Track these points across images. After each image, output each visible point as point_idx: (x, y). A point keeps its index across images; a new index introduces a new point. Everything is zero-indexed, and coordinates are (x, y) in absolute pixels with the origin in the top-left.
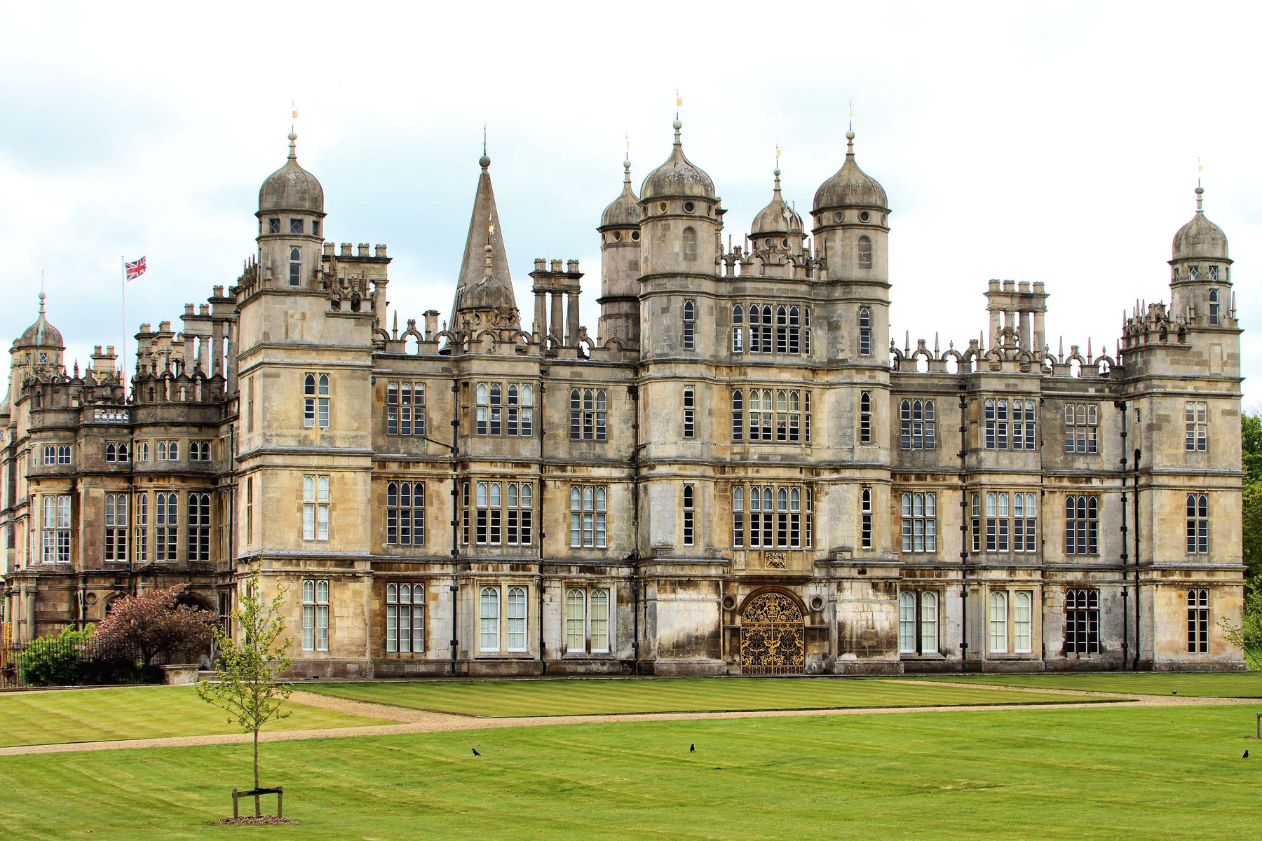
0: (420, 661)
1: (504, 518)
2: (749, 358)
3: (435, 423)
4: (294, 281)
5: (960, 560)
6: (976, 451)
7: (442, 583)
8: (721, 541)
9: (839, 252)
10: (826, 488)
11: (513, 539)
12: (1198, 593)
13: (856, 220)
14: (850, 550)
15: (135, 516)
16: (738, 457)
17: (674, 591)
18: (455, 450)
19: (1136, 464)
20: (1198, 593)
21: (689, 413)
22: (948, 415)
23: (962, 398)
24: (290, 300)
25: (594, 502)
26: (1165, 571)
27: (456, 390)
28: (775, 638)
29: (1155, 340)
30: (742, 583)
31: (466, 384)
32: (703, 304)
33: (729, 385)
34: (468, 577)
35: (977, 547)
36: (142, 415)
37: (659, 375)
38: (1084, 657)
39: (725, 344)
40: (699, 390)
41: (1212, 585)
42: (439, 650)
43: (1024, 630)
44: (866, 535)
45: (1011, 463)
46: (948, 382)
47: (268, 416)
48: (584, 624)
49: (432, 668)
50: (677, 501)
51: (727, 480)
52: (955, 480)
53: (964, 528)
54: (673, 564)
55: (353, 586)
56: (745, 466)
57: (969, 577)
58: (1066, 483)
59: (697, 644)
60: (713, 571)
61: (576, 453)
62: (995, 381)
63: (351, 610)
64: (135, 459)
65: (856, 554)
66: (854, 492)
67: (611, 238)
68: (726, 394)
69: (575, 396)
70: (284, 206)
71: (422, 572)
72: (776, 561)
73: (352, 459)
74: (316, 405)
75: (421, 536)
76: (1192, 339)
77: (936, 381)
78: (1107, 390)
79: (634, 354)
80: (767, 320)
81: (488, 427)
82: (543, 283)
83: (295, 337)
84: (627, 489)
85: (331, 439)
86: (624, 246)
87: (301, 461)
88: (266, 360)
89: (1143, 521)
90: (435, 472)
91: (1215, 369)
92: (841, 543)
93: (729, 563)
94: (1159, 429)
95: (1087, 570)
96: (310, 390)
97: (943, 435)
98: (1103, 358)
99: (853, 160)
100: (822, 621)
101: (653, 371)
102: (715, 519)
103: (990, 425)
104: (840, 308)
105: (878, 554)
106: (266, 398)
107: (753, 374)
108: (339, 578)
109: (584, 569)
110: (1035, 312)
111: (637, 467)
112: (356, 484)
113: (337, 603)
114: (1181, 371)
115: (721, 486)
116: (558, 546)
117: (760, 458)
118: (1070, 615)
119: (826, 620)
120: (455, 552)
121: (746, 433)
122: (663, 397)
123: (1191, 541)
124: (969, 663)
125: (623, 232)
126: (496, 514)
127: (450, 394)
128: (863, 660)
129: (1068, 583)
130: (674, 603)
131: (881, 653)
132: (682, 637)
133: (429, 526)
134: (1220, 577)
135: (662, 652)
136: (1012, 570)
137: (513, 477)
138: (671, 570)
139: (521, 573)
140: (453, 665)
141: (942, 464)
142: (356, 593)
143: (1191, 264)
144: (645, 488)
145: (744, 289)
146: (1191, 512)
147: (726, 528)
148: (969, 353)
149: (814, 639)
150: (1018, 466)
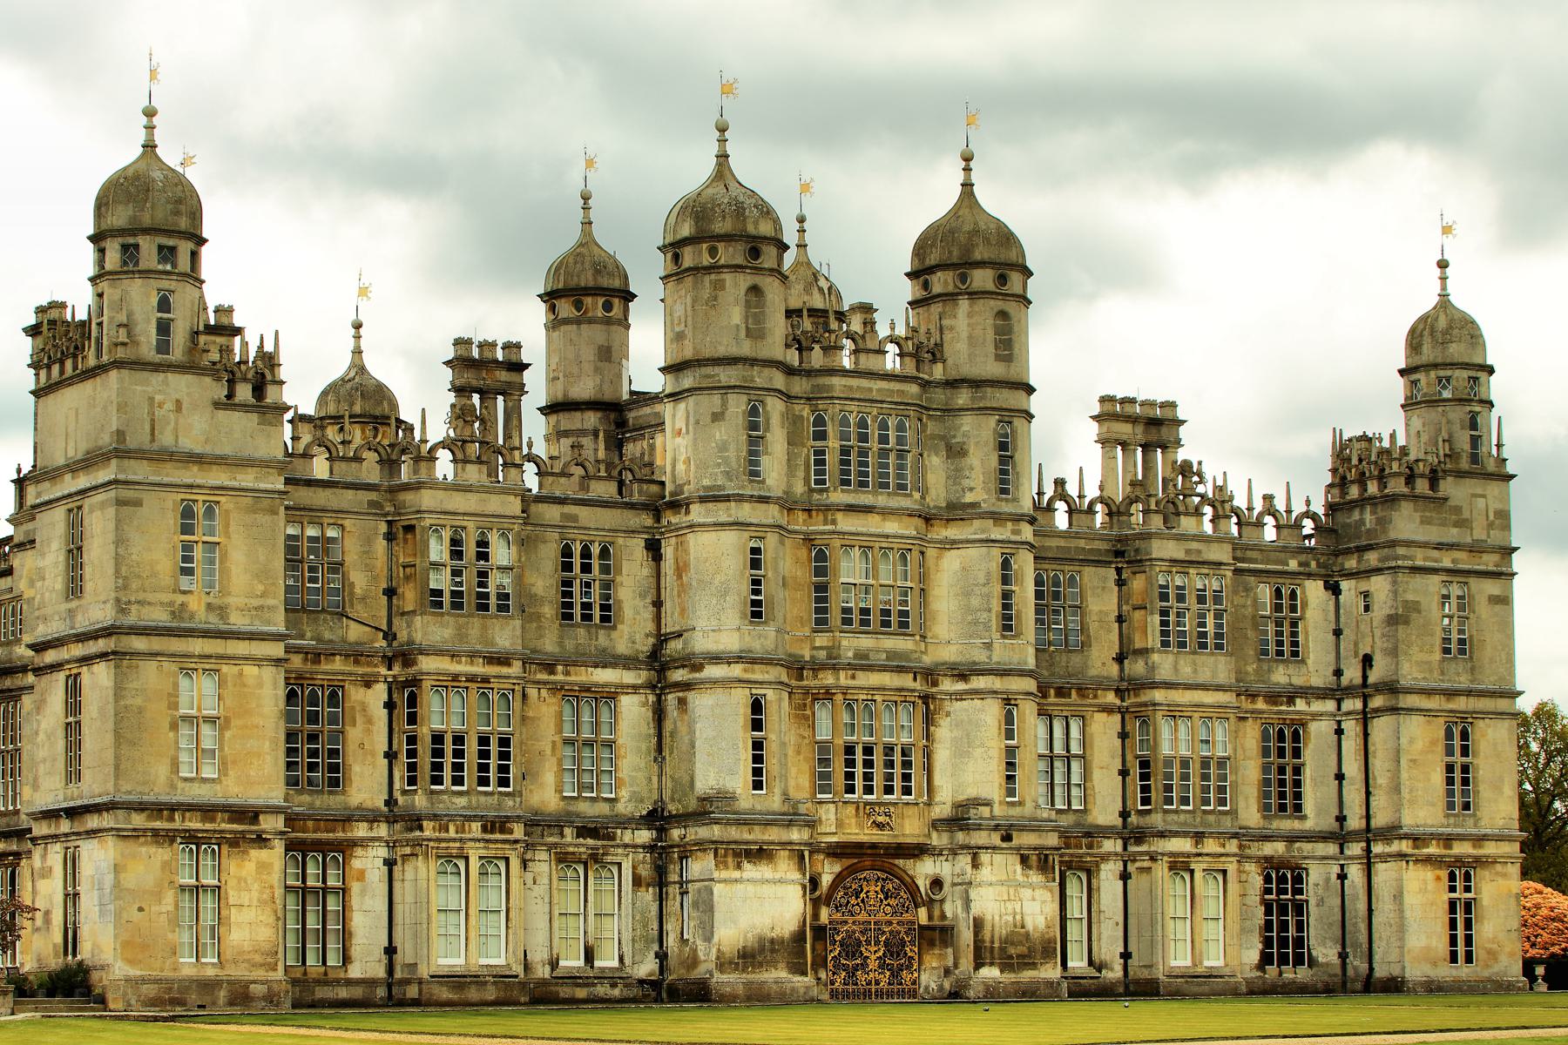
0: (338, 982)
1: (471, 747)
2: (838, 497)
3: (358, 591)
4: (164, 347)
5: (1119, 822)
6: (1144, 652)
7: (371, 852)
8: (798, 787)
9: (964, 335)
10: (949, 706)
11: (484, 781)
12: (1460, 873)
13: (991, 286)
14: (988, 804)
16: (822, 654)
17: (739, 867)
18: (390, 636)
19: (1365, 677)
20: (1460, 873)
21: (756, 582)
22: (1100, 596)
23: (1119, 571)
24: (157, 378)
25: (596, 726)
26: (1417, 839)
27: (390, 537)
28: (877, 943)
29: (1397, 486)
30: (829, 855)
31: (410, 529)
32: (775, 406)
33: (808, 540)
34: (417, 843)
35: (1146, 801)
37: (709, 520)
38: (1289, 974)
39: (801, 474)
40: (771, 543)
41: (1480, 862)
42: (367, 964)
43: (1213, 931)
44: (1010, 778)
45: (1195, 671)
46: (1098, 545)
47: (124, 570)
48: (599, 921)
49: (357, 993)
50: (741, 721)
51: (806, 691)
52: (1111, 698)
53: (1124, 773)
54: (739, 823)
55: (256, 854)
56: (835, 668)
57: (1133, 849)
58: (1260, 705)
59: (773, 951)
60: (795, 835)
61: (570, 645)
62: (1171, 544)
63: (255, 895)
65: (997, 811)
66: (991, 712)
67: (565, 308)
68: (803, 553)
69: (567, 552)
70: (147, 220)
71: (340, 835)
72: (880, 819)
73: (254, 643)
74: (198, 553)
75: (336, 779)
76: (1448, 487)
77: (1082, 543)
78: (1313, 564)
79: (654, 488)
80: (863, 438)
81: (446, 599)
82: (469, 377)
83: (166, 439)
84: (645, 704)
85: (222, 611)
86: (591, 321)
87: (177, 645)
88: (121, 477)
89: (1379, 765)
90: (360, 670)
91: (1479, 533)
92: (971, 792)
93: (812, 824)
94: (1407, 622)
95: (1291, 839)
96: (187, 529)
97: (1093, 627)
98: (1307, 514)
99: (972, 194)
100: (943, 916)
101: (697, 513)
102: (790, 752)
103: (1164, 613)
104: (967, 423)
105: (1028, 810)
106: (120, 541)
107: (846, 523)
108: (234, 843)
109: (584, 831)
110: (1164, 447)
111: (665, 669)
112: (260, 685)
113: (232, 883)
114: (1433, 534)
115: (798, 699)
116: (546, 794)
117: (856, 656)
118: (1268, 912)
119: (949, 914)
120: (390, 802)
121: (835, 617)
122: (712, 553)
123: (1450, 793)
124: (1137, 982)
125: (588, 300)
126: (459, 739)
127: (381, 544)
128: (1009, 977)
129: (1268, 859)
130: (739, 886)
131: (1033, 966)
132: (751, 940)
133: (350, 760)
134: (1490, 849)
135: (723, 964)
136: (1199, 837)
137: (486, 680)
138: (734, 833)
139: (498, 836)
140: (390, 986)
141: (1093, 672)
142: (263, 867)
143: (1442, 373)
144: (682, 702)
145: (830, 388)
146: (1449, 751)
147: (806, 767)
148: (1131, 501)
149: (932, 944)
150: (1204, 676)
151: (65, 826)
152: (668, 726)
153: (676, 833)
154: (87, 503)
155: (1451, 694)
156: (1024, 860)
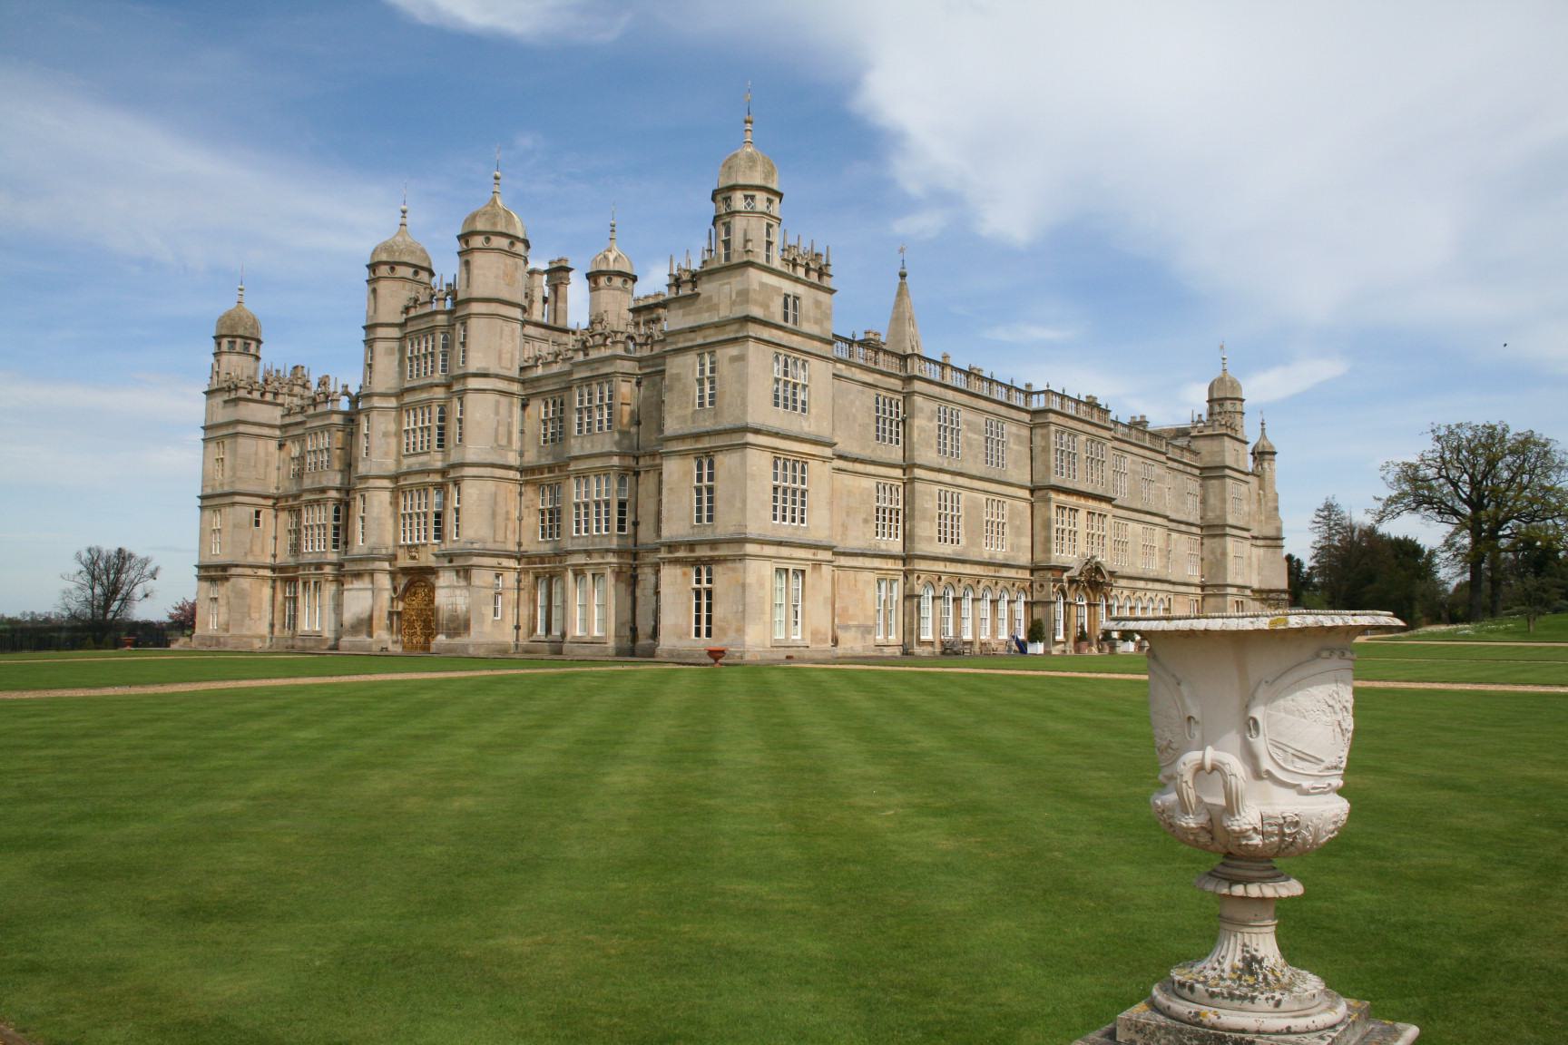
131: (458, 634)
155: (697, 436)
156: (458, 572)
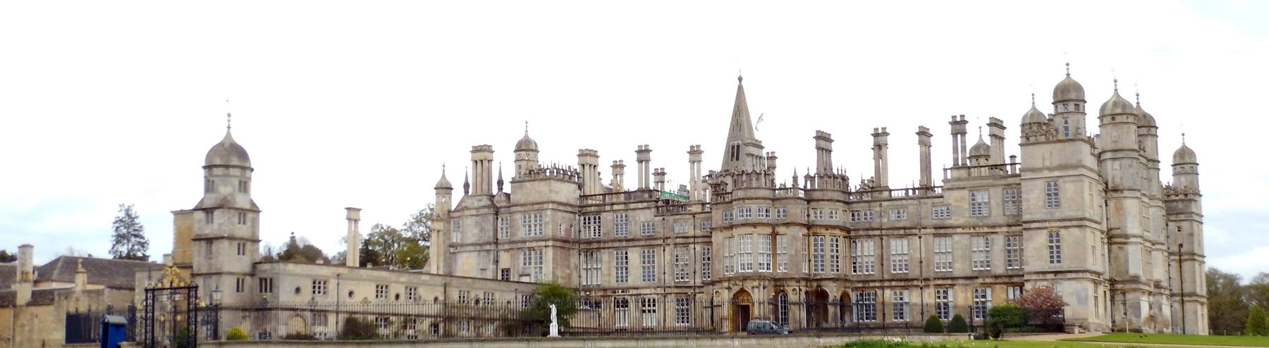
15: (812, 248)
36: (817, 195)
64: (812, 218)
101: (1126, 193)
151: (1052, 276)
152: (1113, 255)
153: (1119, 286)
154: (1061, 180)
